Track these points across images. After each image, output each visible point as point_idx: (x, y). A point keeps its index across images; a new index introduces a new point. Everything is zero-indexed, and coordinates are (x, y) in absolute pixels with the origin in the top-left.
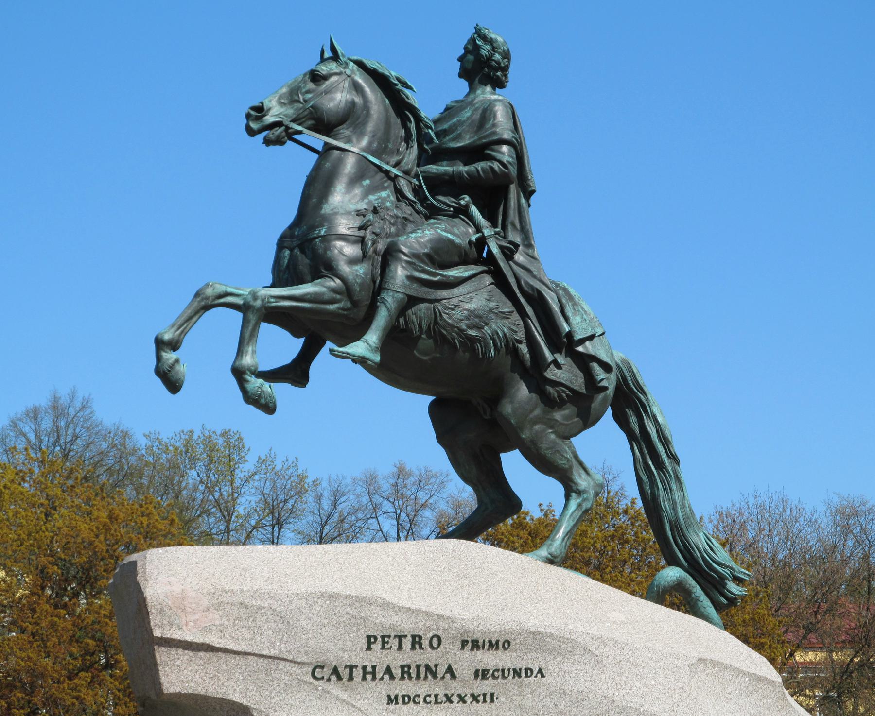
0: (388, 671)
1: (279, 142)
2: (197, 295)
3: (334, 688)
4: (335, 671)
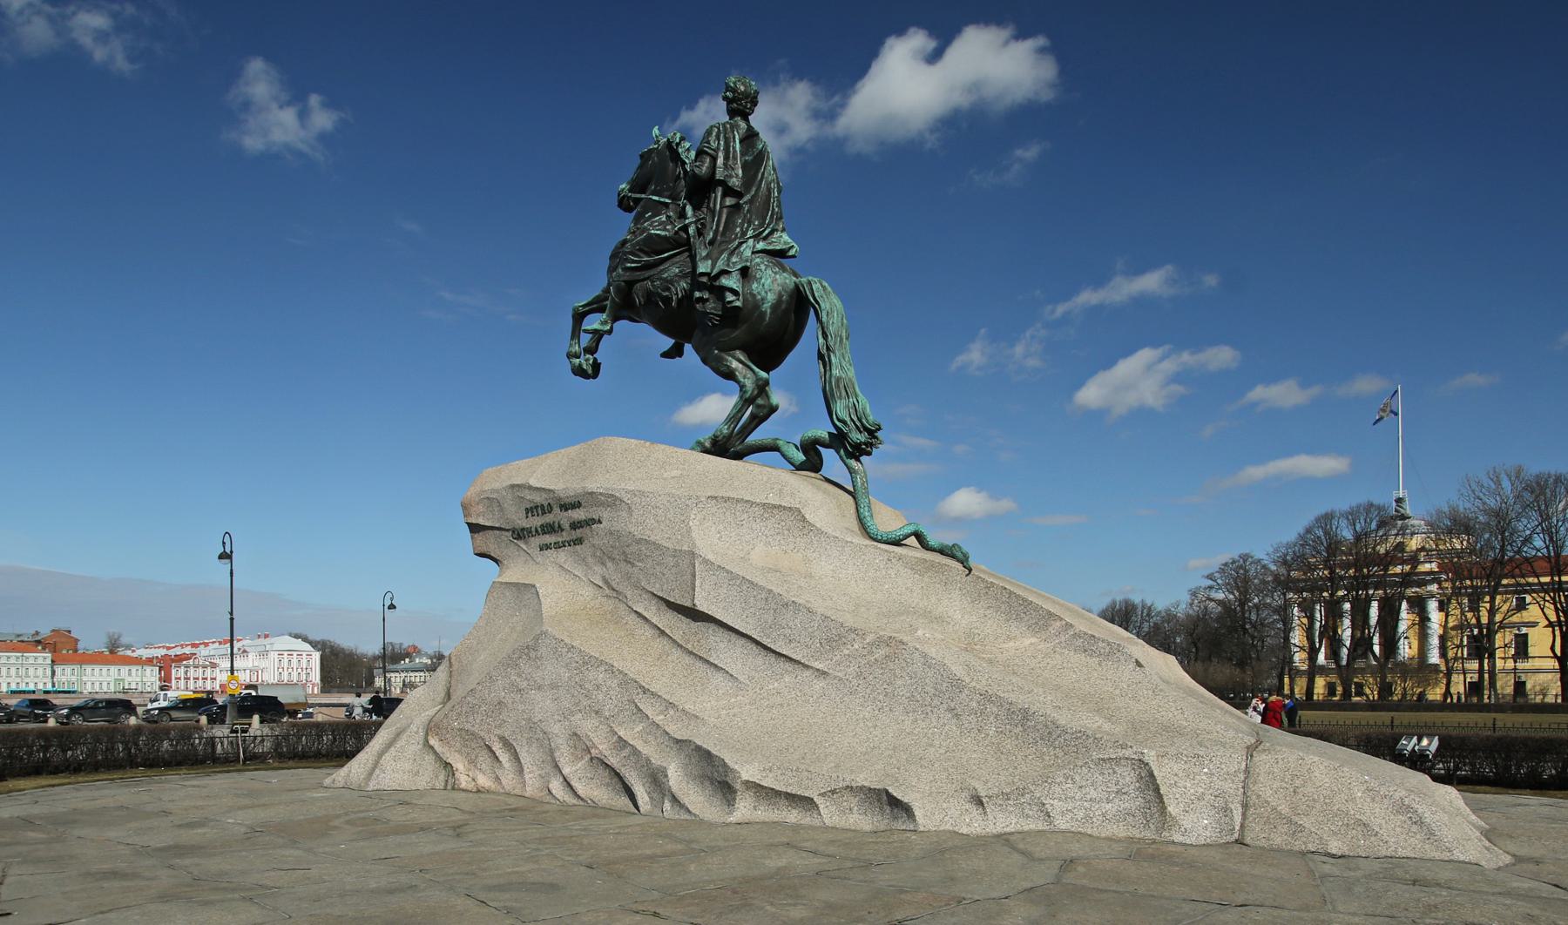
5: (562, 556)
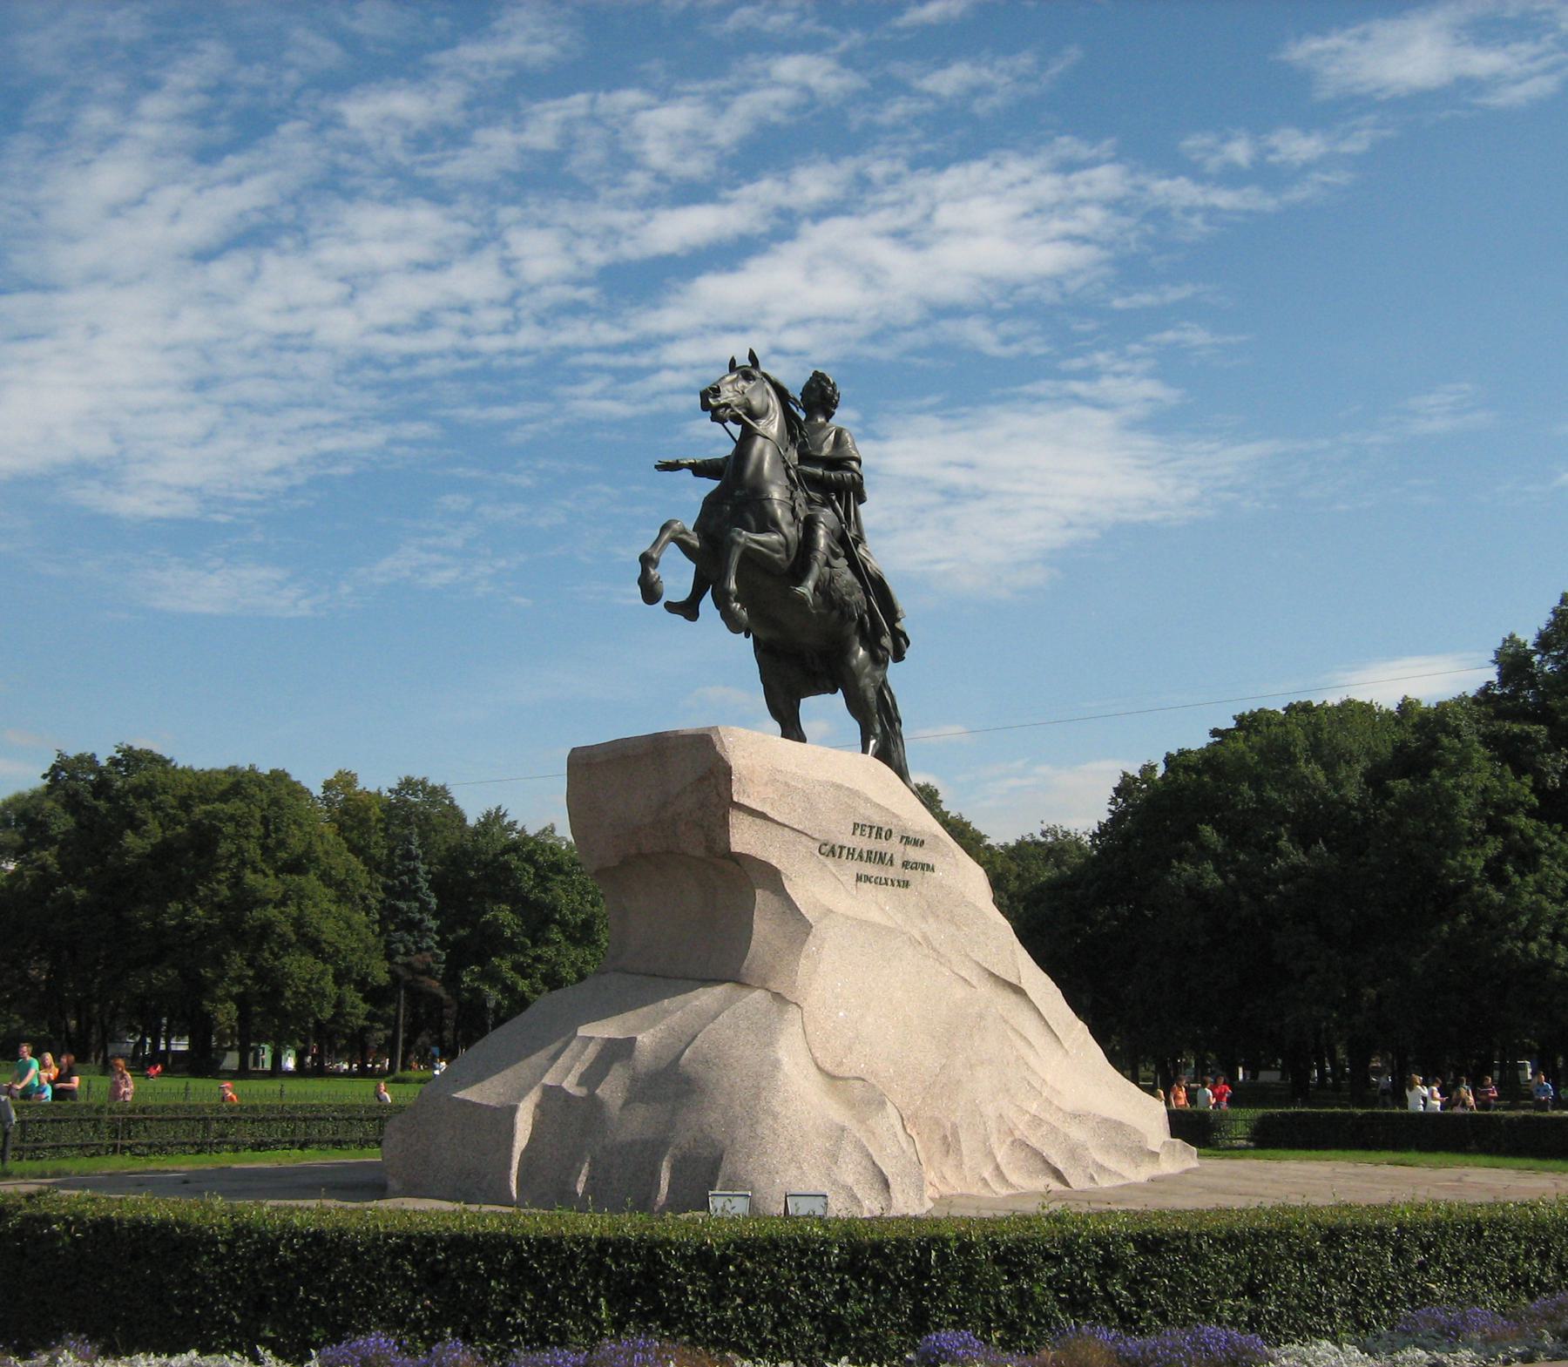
0: (861, 856)
1: (722, 421)
2: (665, 528)
3: (829, 862)
4: (832, 851)
5: (883, 894)
